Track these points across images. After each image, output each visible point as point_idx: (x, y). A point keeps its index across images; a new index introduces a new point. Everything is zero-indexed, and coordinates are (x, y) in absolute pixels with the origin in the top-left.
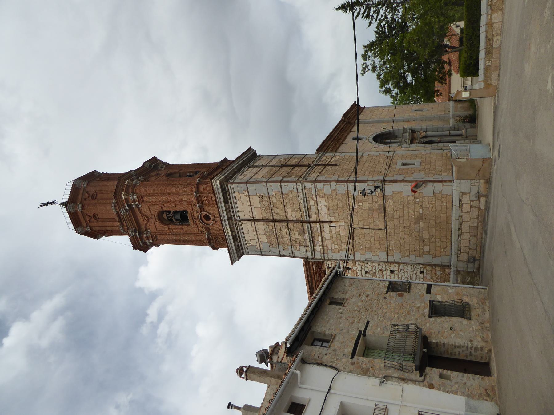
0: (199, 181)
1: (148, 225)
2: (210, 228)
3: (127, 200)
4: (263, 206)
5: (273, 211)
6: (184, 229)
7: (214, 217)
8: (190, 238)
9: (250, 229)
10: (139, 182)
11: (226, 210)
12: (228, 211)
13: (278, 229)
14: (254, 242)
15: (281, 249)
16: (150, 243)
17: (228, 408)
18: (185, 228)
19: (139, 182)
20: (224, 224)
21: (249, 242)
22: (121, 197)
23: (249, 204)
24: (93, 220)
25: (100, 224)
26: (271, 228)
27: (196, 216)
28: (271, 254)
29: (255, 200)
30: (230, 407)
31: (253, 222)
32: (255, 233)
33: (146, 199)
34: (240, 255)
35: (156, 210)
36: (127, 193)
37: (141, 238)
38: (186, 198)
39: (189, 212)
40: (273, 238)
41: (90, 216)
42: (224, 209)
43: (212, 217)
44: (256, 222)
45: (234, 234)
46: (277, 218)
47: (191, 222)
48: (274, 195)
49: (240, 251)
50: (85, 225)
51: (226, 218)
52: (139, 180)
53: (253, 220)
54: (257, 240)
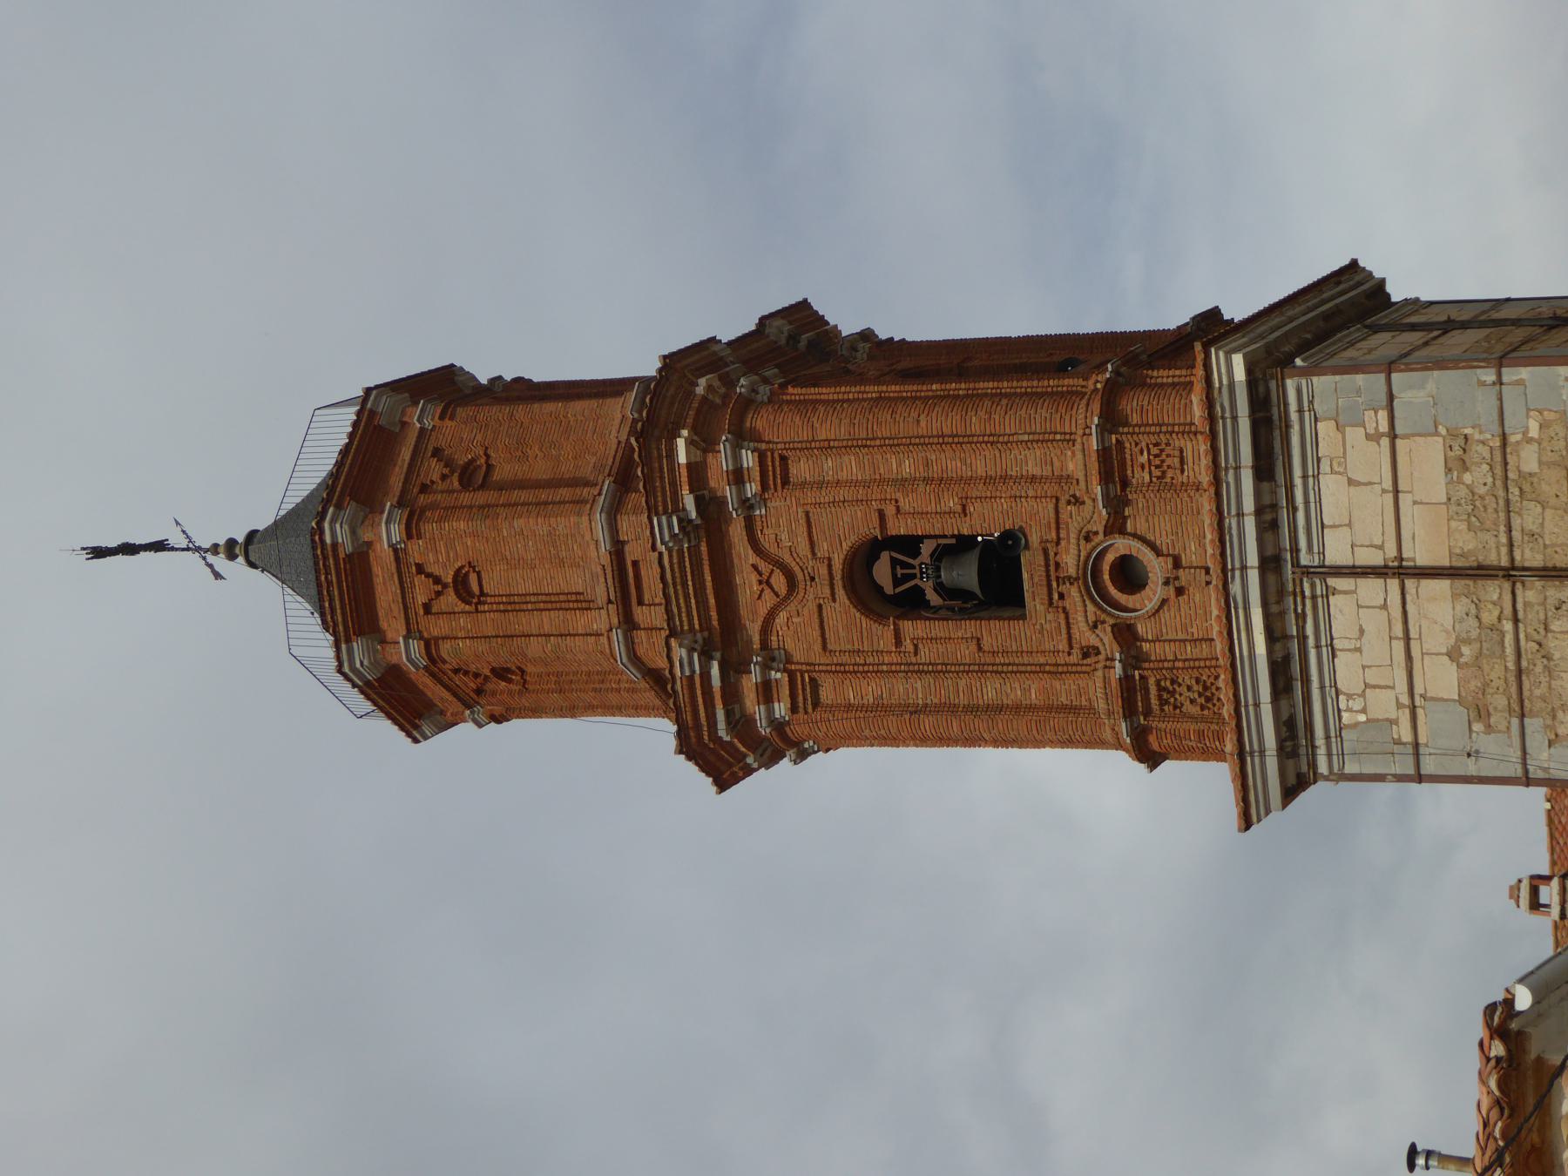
0: (1116, 372)
1: (781, 618)
2: (1140, 629)
3: (697, 472)
4: (1463, 492)
5: (1516, 522)
6: (987, 643)
7: (1177, 564)
8: (1015, 691)
9: (1374, 622)
10: (764, 390)
11: (1259, 512)
12: (1268, 523)
13: (1531, 618)
14: (1384, 704)
15: (1537, 741)
16: (772, 721)
17: (1411, 1166)
18: (995, 633)
19: (764, 390)
20: (1235, 588)
21: (1357, 704)
22: (672, 453)
23: (1388, 484)
24: (450, 599)
25: (489, 622)
26: (1489, 617)
27: (1070, 561)
28: (1471, 768)
29: (1425, 462)
30: (1421, 1161)
31: (1394, 584)
32: (1399, 646)
33: (801, 469)
34: (1292, 780)
35: (847, 527)
36: (704, 442)
37: (732, 695)
38: (1031, 462)
39: (1034, 539)
40: (1498, 671)
41: (437, 580)
42: (1249, 505)
43: (1156, 568)
44: (1410, 584)
45: (1279, 656)
46: (1530, 556)
47: (1035, 601)
48: (1534, 432)
49: (1294, 754)
50: (393, 627)
51: (1253, 559)
52: (766, 381)
53: (1400, 571)
54: (1402, 686)
